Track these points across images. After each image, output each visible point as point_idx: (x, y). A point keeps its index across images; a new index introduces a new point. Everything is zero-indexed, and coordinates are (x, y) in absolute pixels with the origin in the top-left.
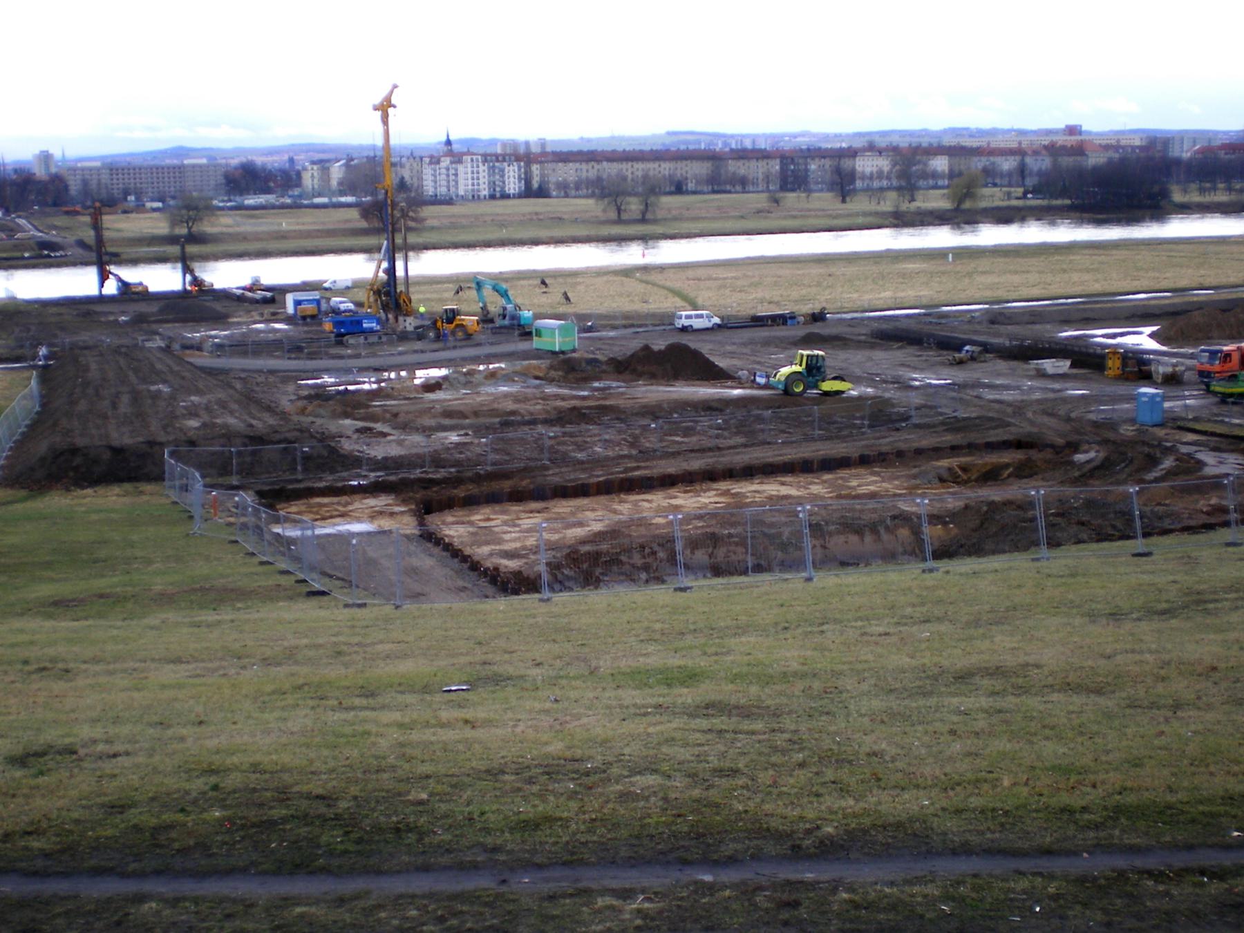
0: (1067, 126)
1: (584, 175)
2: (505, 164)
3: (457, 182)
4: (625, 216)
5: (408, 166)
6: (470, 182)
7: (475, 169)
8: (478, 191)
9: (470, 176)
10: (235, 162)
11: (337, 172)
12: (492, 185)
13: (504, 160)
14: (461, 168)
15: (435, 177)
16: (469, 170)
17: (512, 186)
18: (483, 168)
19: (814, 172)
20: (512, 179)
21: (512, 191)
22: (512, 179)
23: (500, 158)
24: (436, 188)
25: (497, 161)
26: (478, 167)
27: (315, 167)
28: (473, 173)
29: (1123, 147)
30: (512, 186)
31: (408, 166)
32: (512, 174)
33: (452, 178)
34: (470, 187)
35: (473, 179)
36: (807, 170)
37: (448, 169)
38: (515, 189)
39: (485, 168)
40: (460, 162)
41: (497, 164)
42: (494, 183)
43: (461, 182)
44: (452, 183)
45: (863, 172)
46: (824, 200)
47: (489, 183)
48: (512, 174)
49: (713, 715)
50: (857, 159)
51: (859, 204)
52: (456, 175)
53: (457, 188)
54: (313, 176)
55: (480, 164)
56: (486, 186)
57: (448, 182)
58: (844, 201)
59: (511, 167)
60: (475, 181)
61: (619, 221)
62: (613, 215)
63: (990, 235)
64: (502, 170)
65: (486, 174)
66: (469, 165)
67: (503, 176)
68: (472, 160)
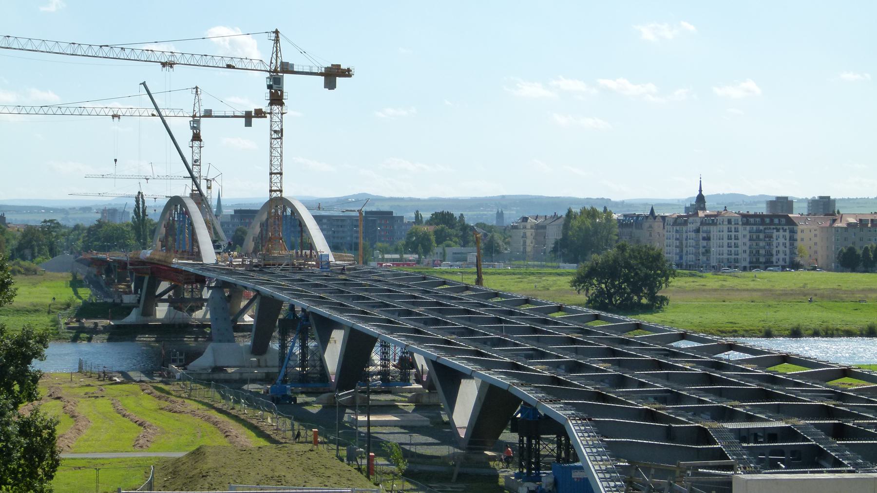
7: (733, 234)
9: (726, 242)
14: (714, 230)
15: (681, 243)
16: (725, 234)
17: (781, 256)
18: (744, 232)
20: (781, 248)
22: (781, 248)
23: (767, 220)
24: (681, 258)
25: (763, 223)
26: (736, 231)
28: (729, 238)
30: (781, 256)
32: (781, 240)
33: (705, 243)
34: (725, 256)
38: (784, 260)
39: (747, 233)
41: (761, 228)
42: (758, 252)
47: (751, 252)
52: (708, 239)
55: (740, 228)
56: (746, 256)
59: (781, 233)
60: (733, 249)
65: (746, 240)
66: (725, 228)
67: (769, 244)
68: (729, 222)
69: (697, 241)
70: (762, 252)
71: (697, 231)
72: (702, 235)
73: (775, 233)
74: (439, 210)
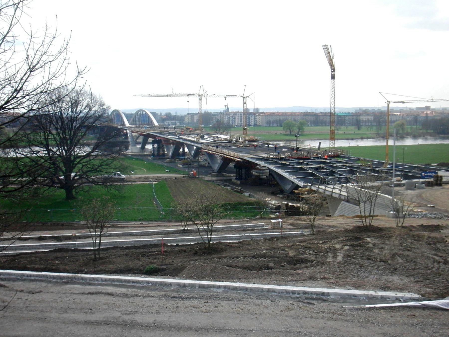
0: (425, 107)
1: (275, 119)
2: (250, 116)
3: (235, 121)
4: (292, 133)
5: (219, 115)
6: (239, 121)
8: (242, 124)
9: (239, 119)
10: (163, 113)
11: (196, 118)
12: (246, 121)
13: (250, 114)
16: (239, 117)
17: (252, 122)
19: (347, 120)
20: (252, 121)
21: (252, 124)
22: (252, 121)
25: (248, 114)
27: (189, 115)
29: (445, 113)
30: (252, 122)
31: (219, 115)
32: (252, 119)
33: (234, 119)
35: (240, 120)
36: (345, 120)
37: (232, 117)
40: (236, 114)
43: (237, 121)
44: (234, 121)
45: (363, 120)
46: (352, 129)
48: (252, 119)
49: (169, 179)
50: (361, 116)
51: (364, 130)
52: (235, 118)
53: (235, 123)
54: (188, 118)
55: (243, 116)
57: (232, 121)
58: (359, 129)
61: (291, 135)
62: (288, 133)
63: (409, 142)
64: (250, 117)
67: (250, 119)
68: (240, 114)
69: (232, 119)
70: (248, 122)
71: (232, 117)
72: (234, 117)
73: (251, 117)
74: (167, 112)
